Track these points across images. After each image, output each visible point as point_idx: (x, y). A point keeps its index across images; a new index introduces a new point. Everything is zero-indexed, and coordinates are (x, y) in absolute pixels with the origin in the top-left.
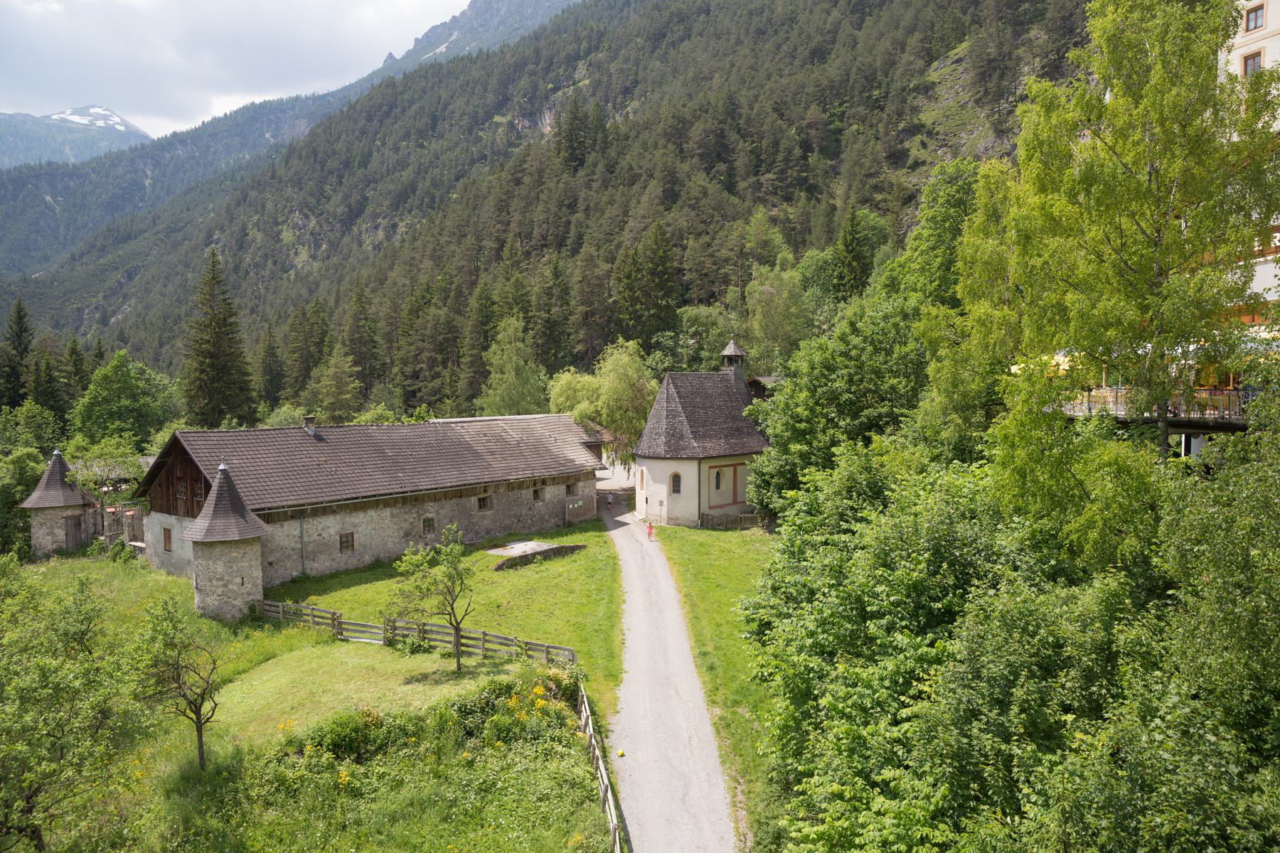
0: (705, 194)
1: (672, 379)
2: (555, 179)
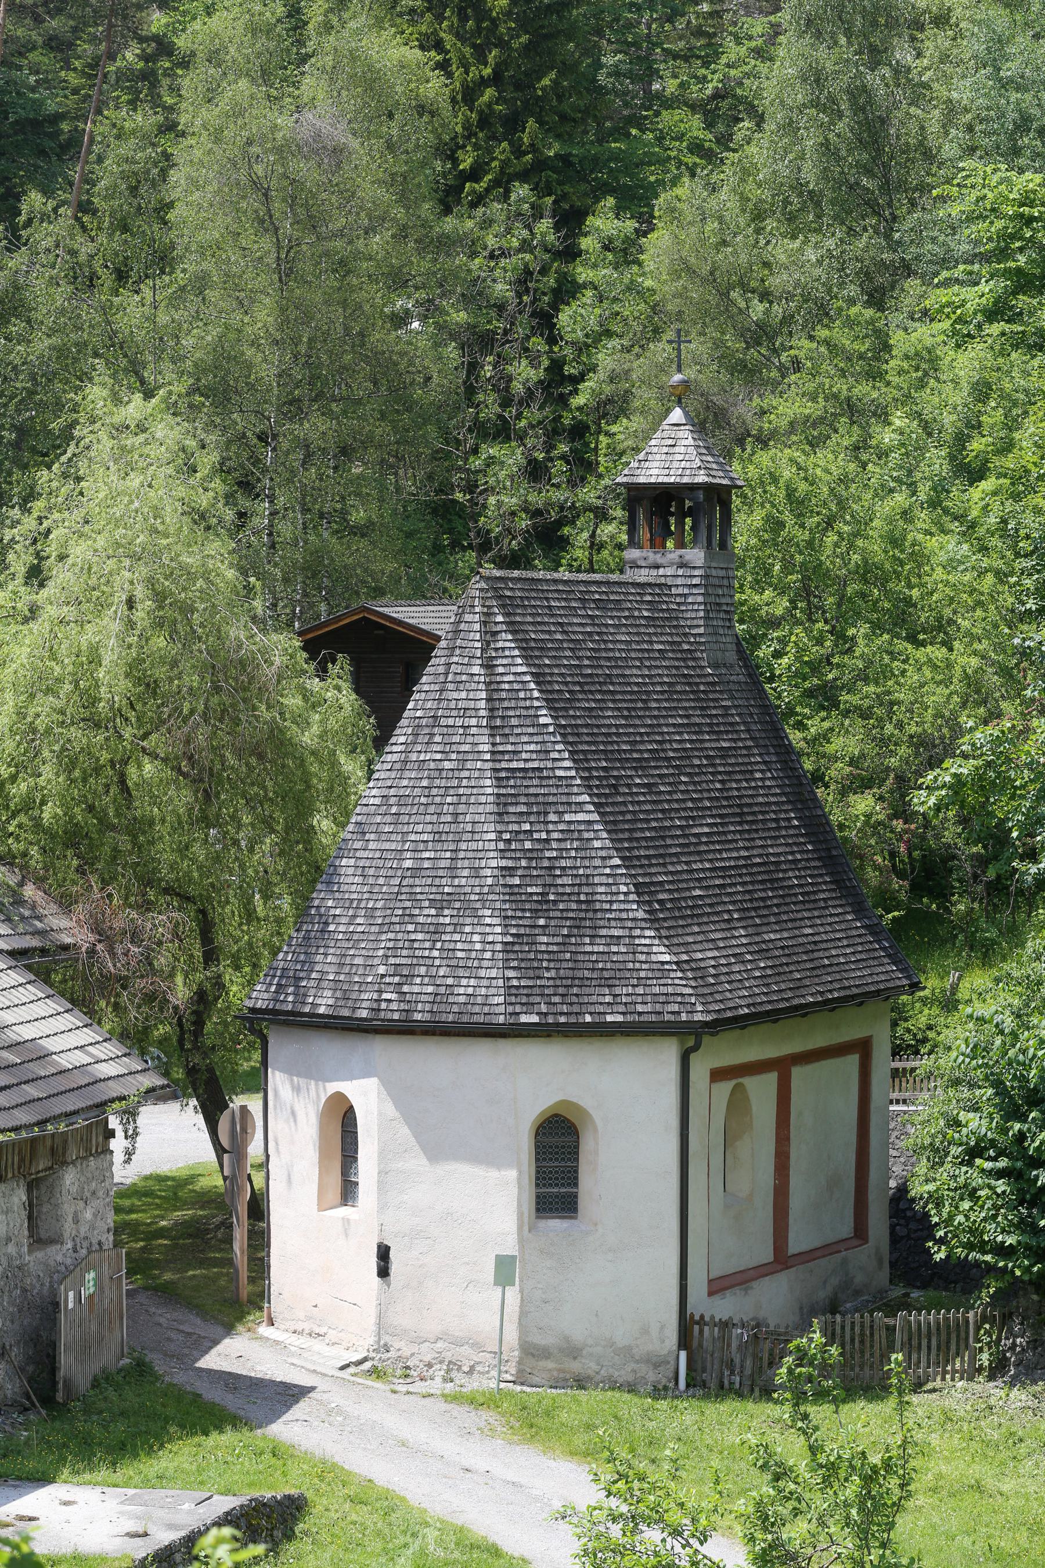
1: (508, 605)
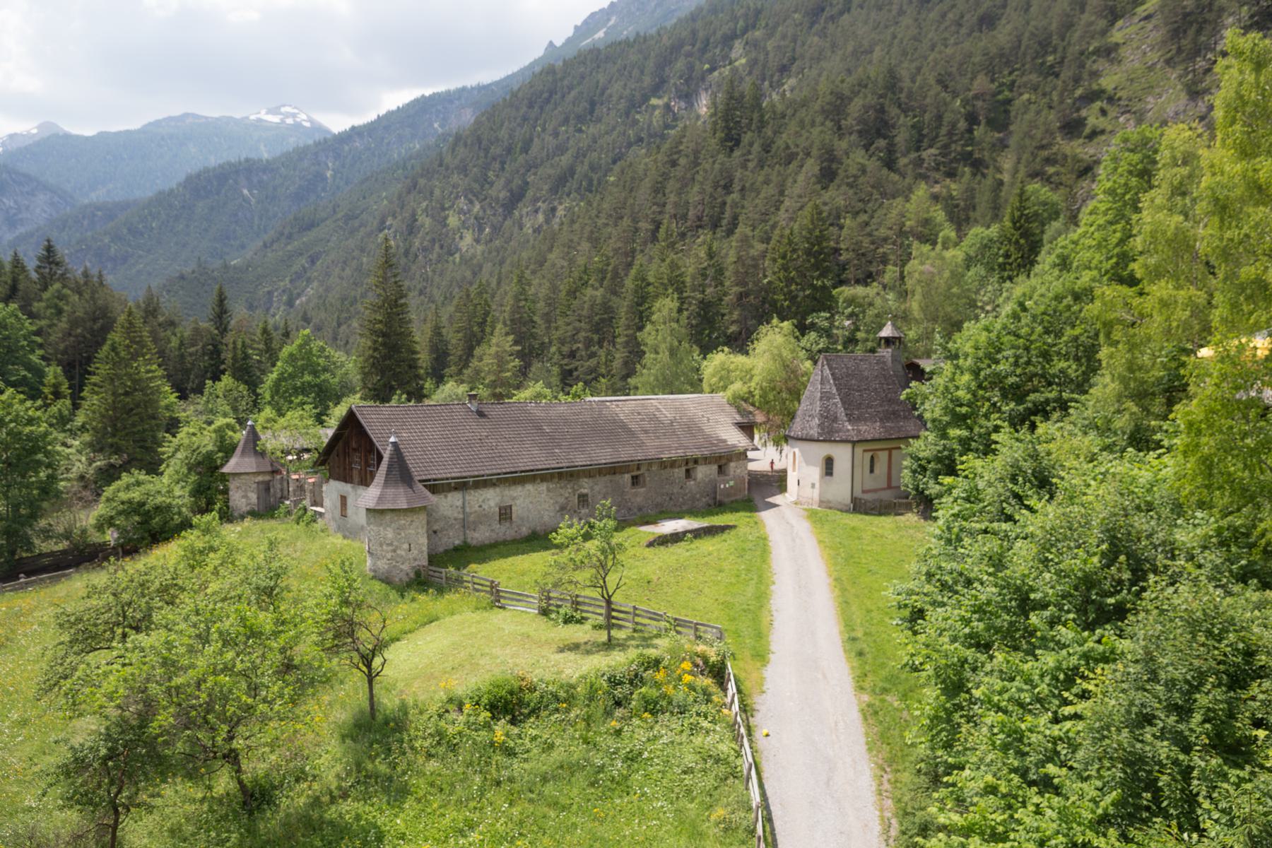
0: (864, 171)
2: (711, 160)
